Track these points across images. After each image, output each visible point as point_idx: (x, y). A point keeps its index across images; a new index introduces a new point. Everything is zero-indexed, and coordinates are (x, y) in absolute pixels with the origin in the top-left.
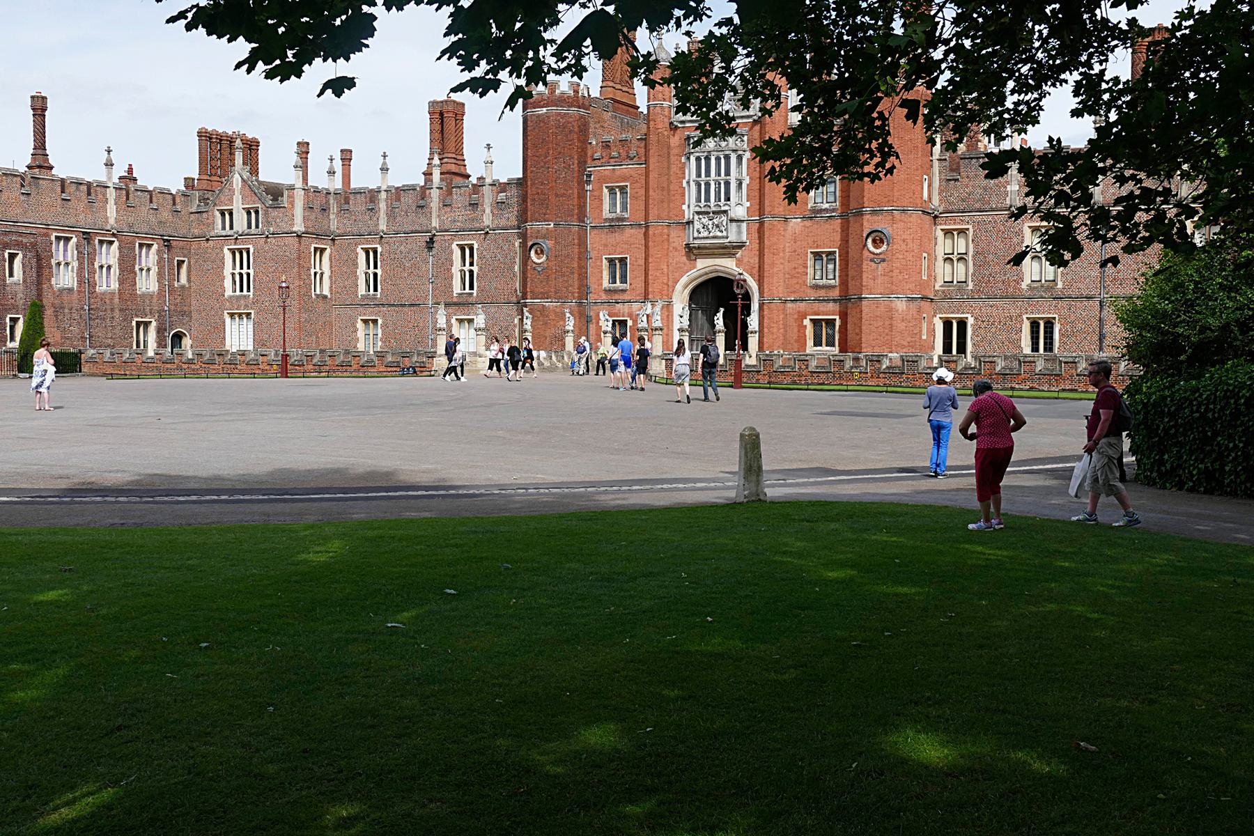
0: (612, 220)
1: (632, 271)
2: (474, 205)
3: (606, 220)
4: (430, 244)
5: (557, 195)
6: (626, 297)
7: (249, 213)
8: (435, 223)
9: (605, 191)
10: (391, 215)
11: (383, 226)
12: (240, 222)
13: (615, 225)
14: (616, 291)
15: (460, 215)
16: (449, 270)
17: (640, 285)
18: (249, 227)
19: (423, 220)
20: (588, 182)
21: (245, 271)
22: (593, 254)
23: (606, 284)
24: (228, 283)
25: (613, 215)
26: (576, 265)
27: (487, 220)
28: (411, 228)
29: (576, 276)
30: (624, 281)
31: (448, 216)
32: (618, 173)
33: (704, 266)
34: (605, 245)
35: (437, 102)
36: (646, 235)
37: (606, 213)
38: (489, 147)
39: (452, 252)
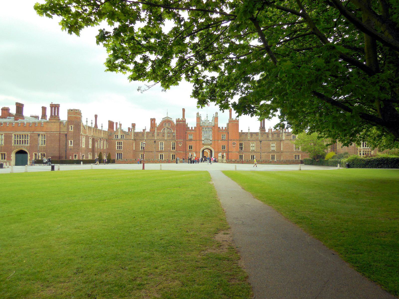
2: (163, 136)
4: (155, 142)
6: (192, 151)
7: (121, 135)
8: (156, 138)
10: (147, 137)
11: (145, 138)
12: (119, 137)
13: (191, 140)
14: (190, 150)
15: (161, 137)
18: (121, 138)
19: (153, 138)
21: (119, 145)
23: (189, 149)
24: (117, 148)
27: (166, 138)
31: (158, 138)
33: (205, 147)
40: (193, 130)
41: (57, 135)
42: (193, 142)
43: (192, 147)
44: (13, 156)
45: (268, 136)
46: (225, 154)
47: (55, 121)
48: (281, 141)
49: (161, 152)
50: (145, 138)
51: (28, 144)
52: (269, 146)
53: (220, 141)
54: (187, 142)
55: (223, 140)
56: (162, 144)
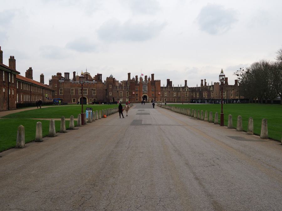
2: (122, 88)
4: (118, 92)
31: (119, 89)
33: (144, 95)
41: (102, 89)
43: (137, 94)
44: (79, 100)
45: (172, 89)
46: (154, 99)
47: (100, 82)
48: (178, 92)
49: (121, 97)
51: (86, 94)
52: (173, 94)
53: (151, 92)
55: (152, 91)
56: (121, 93)
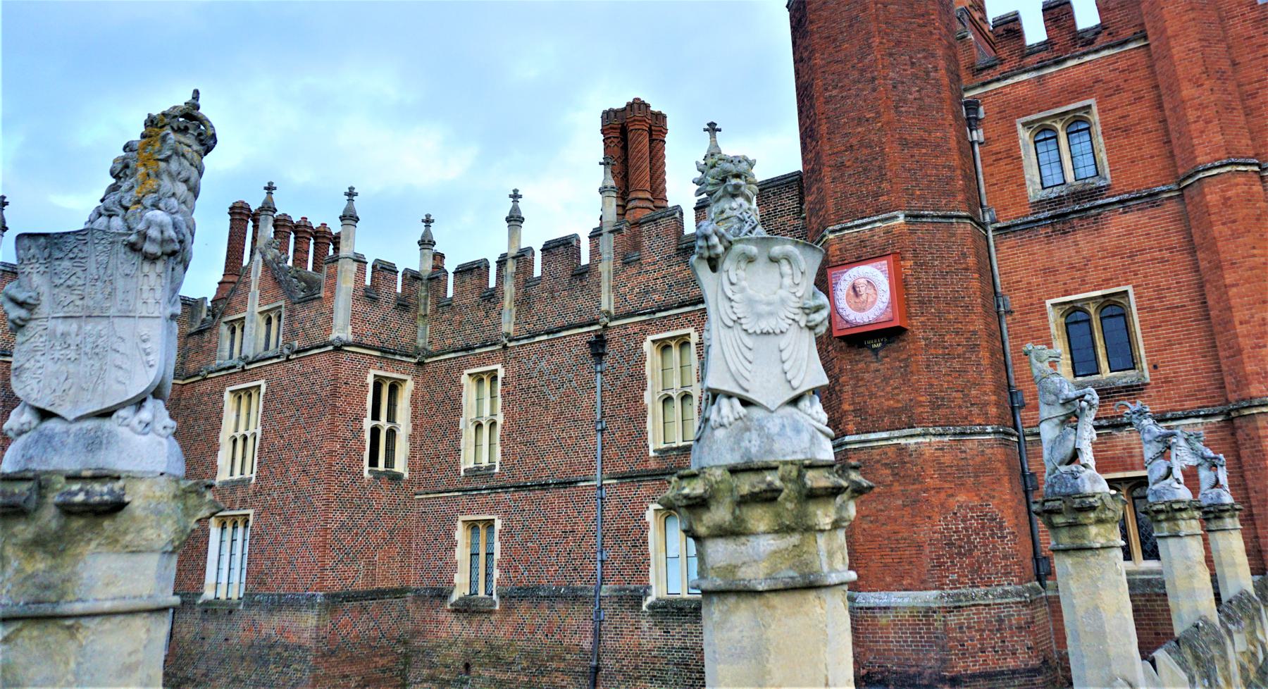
0: (1059, 200)
1: (1149, 327)
3: (1040, 204)
5: (904, 143)
9: (1024, 135)
13: (1072, 210)
16: (638, 399)
17: (1187, 365)
20: (973, 123)
22: (1014, 301)
25: (1064, 191)
26: (979, 325)
28: (560, 322)
29: (984, 354)
30: (1124, 357)
32: (1055, 84)
34: (1049, 271)
35: (616, 112)
36: (1184, 221)
37: (1034, 191)
38: (712, 128)
39: (642, 359)
40: (1087, 40)
42: (1119, 224)
50: (508, 326)
54: (1014, 262)
